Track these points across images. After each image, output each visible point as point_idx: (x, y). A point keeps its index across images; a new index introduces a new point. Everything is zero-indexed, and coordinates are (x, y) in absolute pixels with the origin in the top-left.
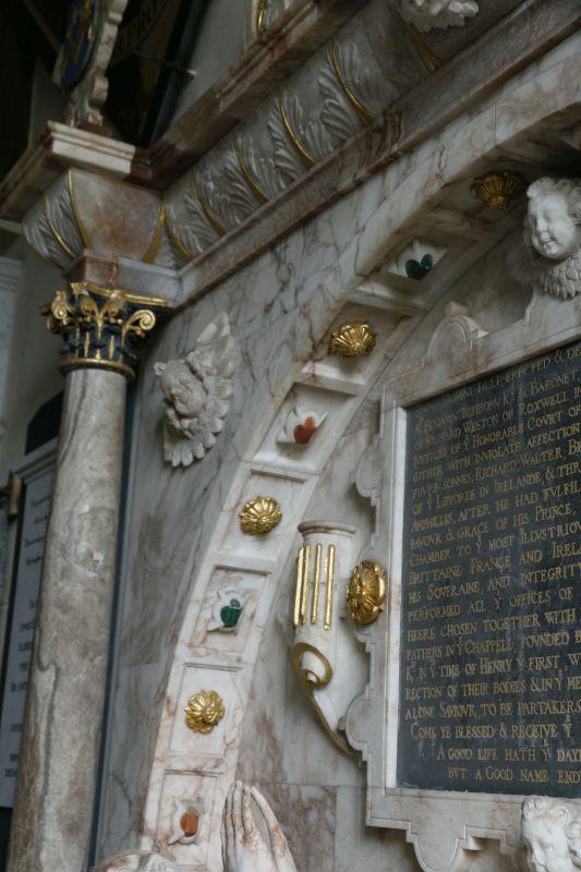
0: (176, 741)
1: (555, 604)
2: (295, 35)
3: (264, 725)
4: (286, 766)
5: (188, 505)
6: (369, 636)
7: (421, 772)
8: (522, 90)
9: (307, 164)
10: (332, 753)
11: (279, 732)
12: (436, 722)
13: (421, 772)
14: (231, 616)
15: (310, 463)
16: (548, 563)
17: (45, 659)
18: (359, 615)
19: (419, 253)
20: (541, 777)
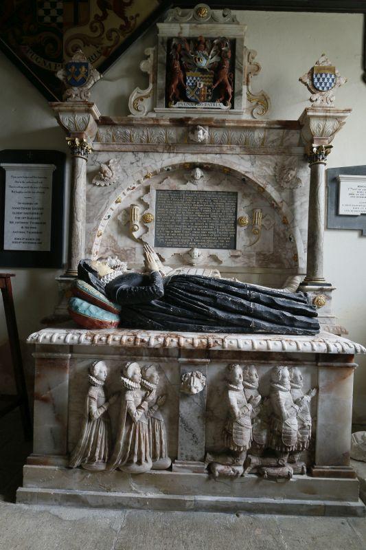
0: (97, 240)
1: (190, 224)
2: (162, 123)
3: (110, 237)
4: (119, 244)
5: (102, 194)
6: (148, 225)
7: (159, 244)
8: (204, 156)
9: (148, 142)
10: (134, 242)
11: (116, 238)
12: (164, 239)
13: (159, 244)
14: (109, 217)
15: (130, 191)
16: (189, 219)
17: (79, 219)
18: (145, 220)
19: (170, 168)
20: (186, 246)
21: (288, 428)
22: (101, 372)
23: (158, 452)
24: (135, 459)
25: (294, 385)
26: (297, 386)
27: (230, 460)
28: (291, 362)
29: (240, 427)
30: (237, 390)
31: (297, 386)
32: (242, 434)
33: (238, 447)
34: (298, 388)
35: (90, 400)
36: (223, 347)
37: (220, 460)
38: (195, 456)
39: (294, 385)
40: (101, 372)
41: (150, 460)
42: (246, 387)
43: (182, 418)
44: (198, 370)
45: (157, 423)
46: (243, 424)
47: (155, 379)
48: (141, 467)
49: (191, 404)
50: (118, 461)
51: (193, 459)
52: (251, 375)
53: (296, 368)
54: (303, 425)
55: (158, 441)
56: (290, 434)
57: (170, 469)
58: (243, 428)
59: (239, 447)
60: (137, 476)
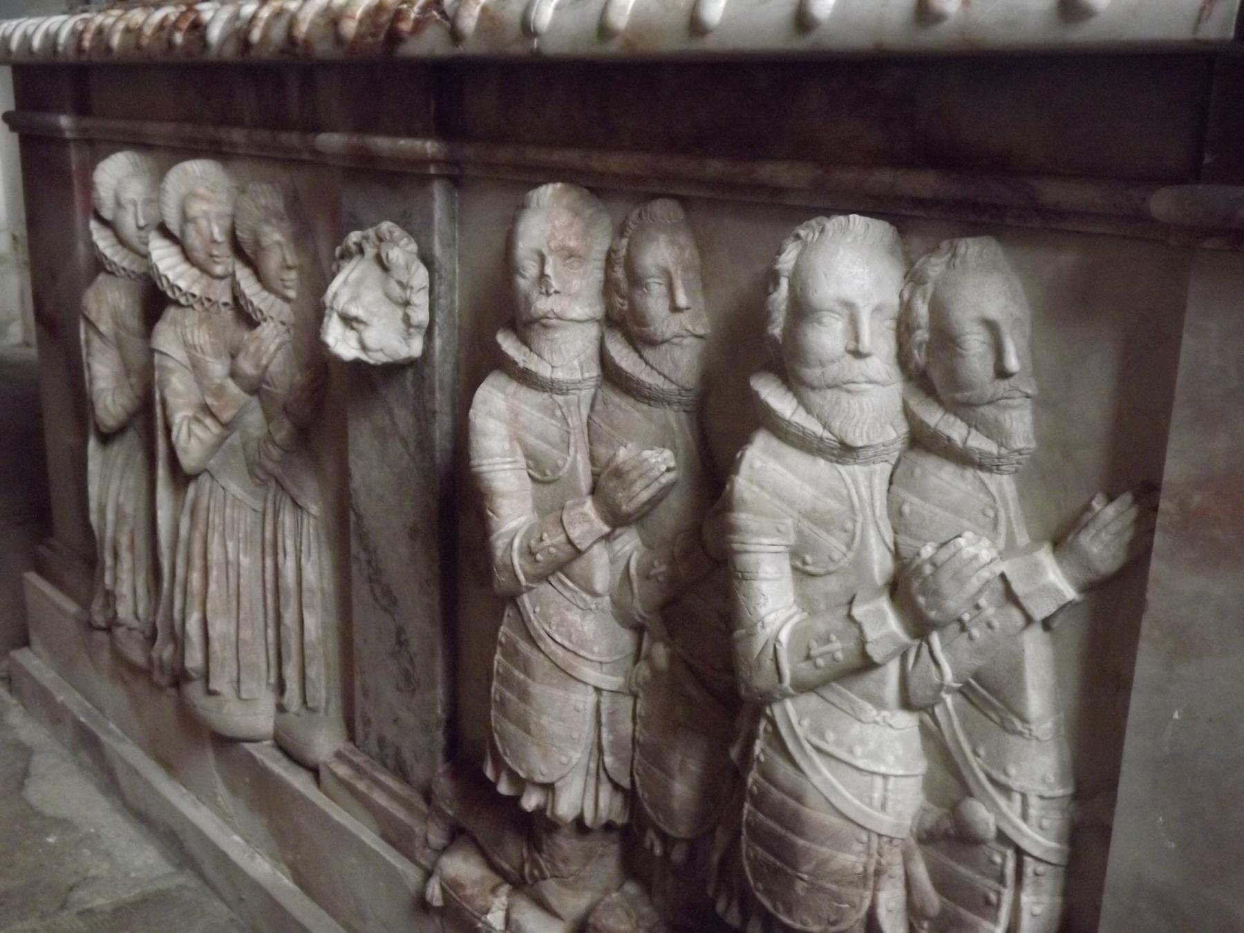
21: (782, 769)
22: (119, 204)
23: (291, 672)
24: (194, 659)
25: (934, 417)
26: (956, 430)
27: (512, 851)
28: (924, 183)
29: (524, 646)
30: (526, 378)
31: (956, 430)
32: (524, 695)
33: (514, 777)
34: (963, 458)
35: (86, 333)
36: (455, 35)
37: (481, 827)
38: (408, 755)
39: (934, 417)
40: (119, 204)
41: (266, 702)
42: (611, 375)
43: (359, 517)
44: (404, 222)
45: (287, 519)
46: (536, 623)
47: (272, 262)
48: (210, 702)
49: (381, 435)
50: (166, 652)
51: (401, 772)
52: (636, 280)
53: (972, 249)
54: (954, 811)
55: (289, 617)
56: (795, 823)
57: (314, 771)
58: (534, 655)
59: (520, 783)
60: (225, 743)
